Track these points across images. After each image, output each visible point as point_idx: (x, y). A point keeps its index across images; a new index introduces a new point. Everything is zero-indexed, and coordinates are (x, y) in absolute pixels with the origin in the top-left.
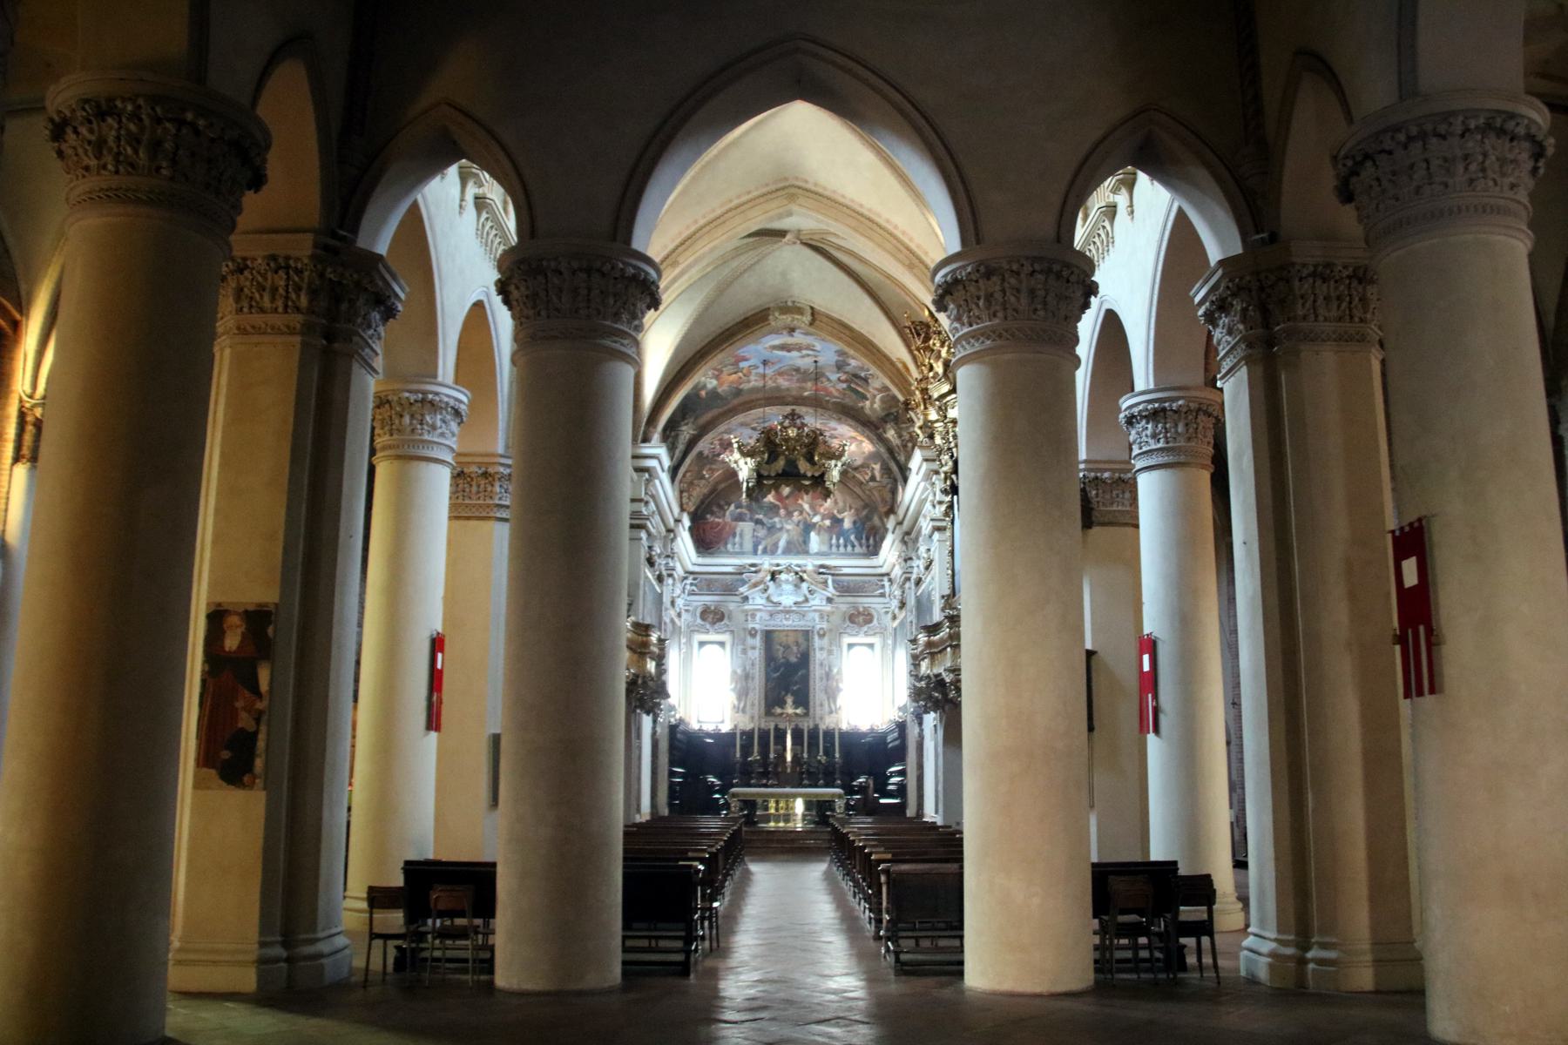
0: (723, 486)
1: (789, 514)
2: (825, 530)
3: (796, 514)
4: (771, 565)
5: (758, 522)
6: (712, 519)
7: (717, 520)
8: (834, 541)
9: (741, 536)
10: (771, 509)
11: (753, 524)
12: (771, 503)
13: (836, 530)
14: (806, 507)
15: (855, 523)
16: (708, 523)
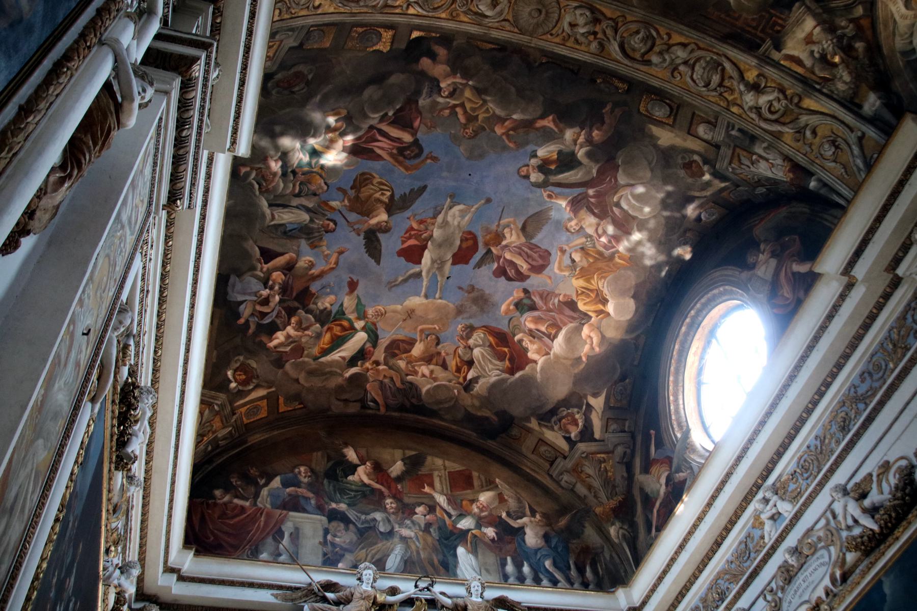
0: (256, 438)
1: (407, 510)
2: (485, 544)
3: (420, 510)
4: (383, 591)
5: (333, 516)
6: (227, 498)
7: (236, 501)
8: (510, 568)
9: (296, 536)
10: (364, 495)
11: (324, 519)
12: (365, 485)
13: (510, 547)
14: (441, 500)
15: (546, 537)
16: (215, 504)
